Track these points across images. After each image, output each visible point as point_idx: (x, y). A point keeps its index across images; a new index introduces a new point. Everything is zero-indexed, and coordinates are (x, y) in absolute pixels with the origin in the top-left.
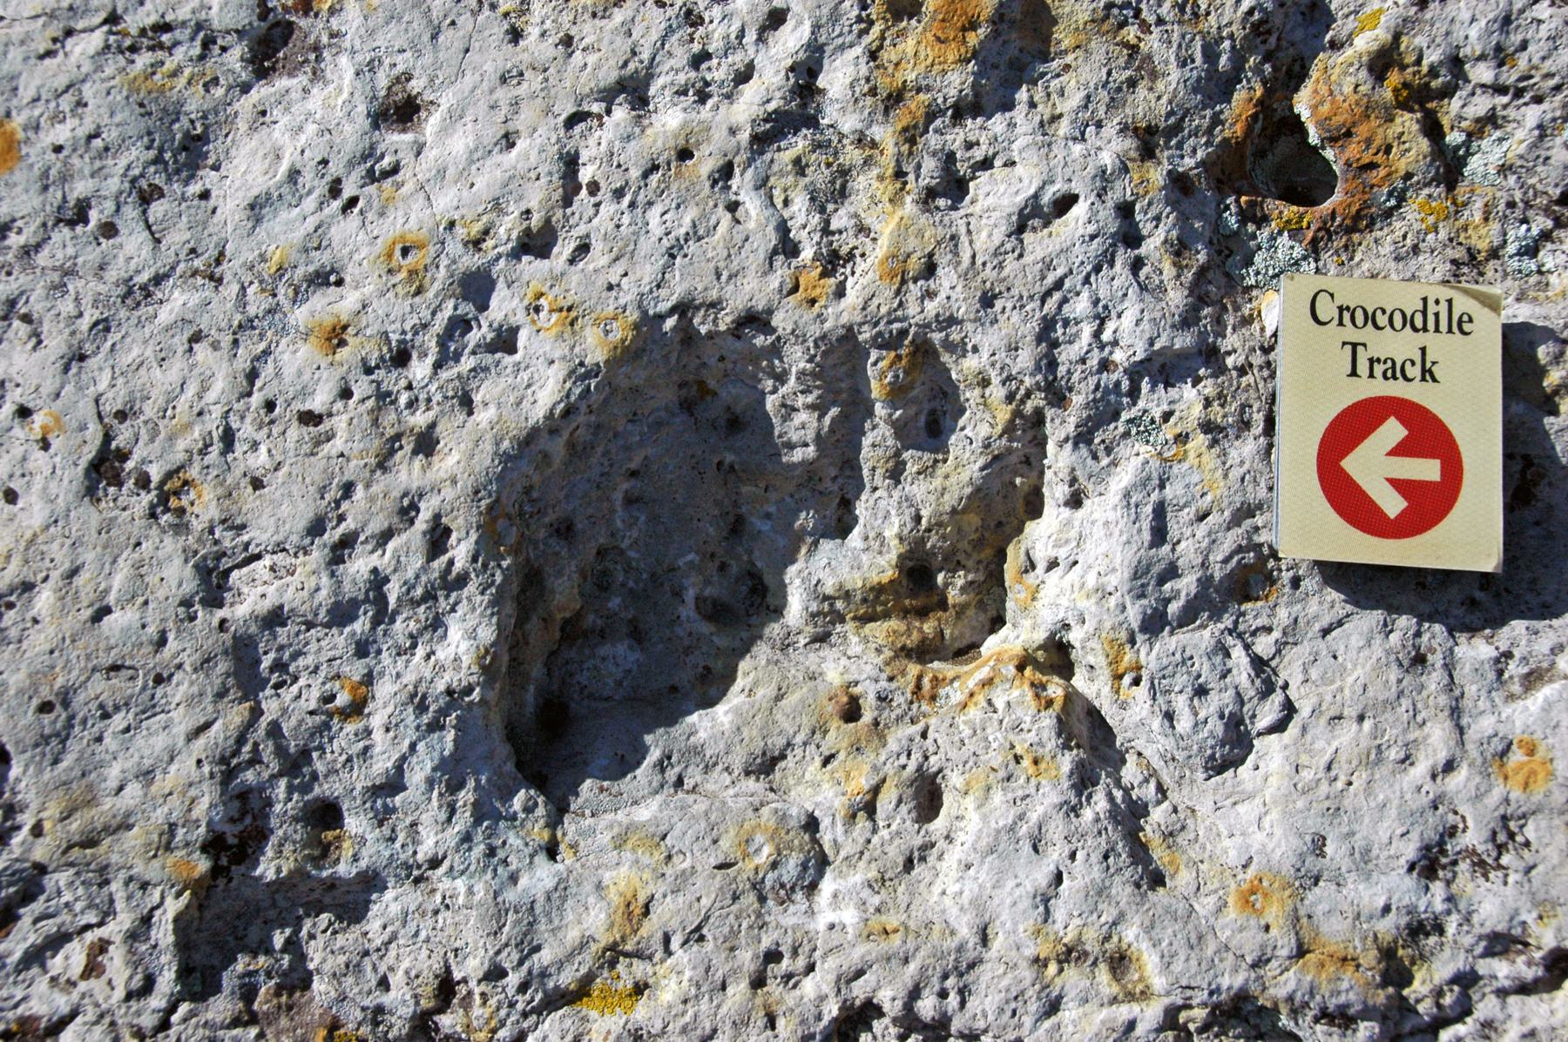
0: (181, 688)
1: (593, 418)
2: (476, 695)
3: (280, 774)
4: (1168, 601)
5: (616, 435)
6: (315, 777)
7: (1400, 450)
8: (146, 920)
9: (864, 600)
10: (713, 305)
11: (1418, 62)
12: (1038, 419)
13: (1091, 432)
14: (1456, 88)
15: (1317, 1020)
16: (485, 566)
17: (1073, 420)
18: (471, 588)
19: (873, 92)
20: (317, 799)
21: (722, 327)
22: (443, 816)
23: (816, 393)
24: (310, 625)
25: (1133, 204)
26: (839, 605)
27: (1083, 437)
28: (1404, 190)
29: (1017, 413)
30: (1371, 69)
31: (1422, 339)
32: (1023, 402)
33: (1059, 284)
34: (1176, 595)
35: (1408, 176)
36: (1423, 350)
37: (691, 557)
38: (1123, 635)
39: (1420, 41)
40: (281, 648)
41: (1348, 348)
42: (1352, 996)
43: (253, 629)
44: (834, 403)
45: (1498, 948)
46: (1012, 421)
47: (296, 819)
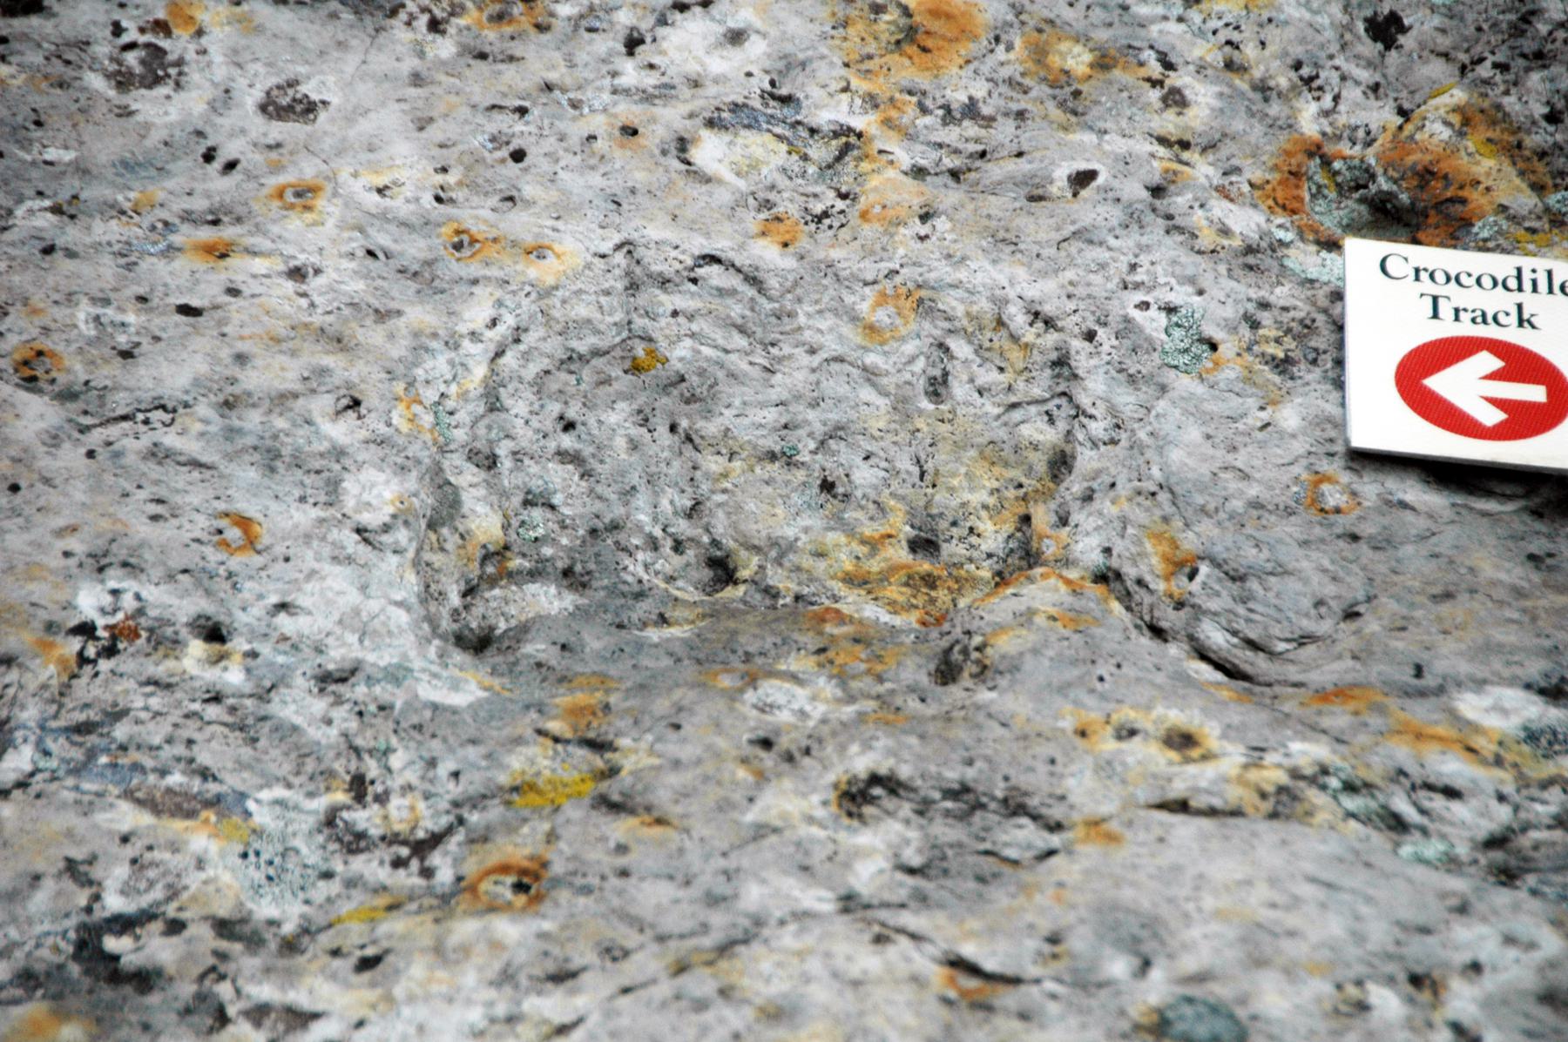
7: (1494, 376)
31: (1517, 297)
36: (1520, 307)
41: (1430, 300)
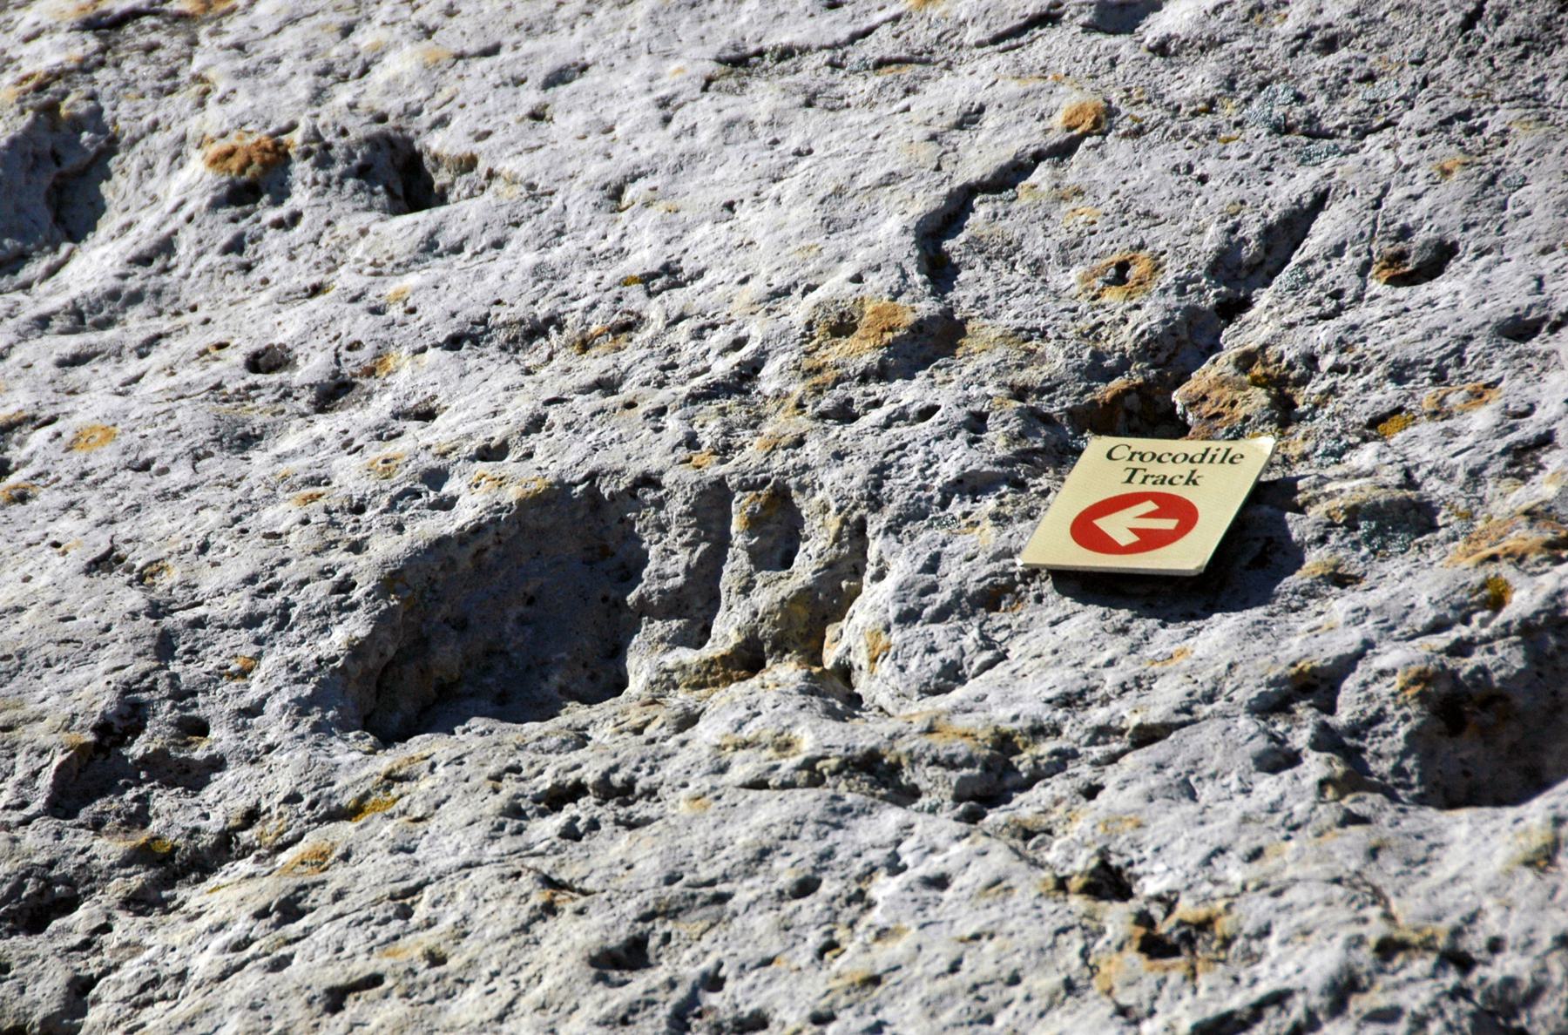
0: (113, 649)
1: (501, 550)
2: (339, 664)
3: (169, 697)
4: (925, 606)
5: (519, 567)
6: (195, 705)
8: (35, 774)
9: (698, 672)
10: (617, 472)
11: (1280, 360)
12: (862, 524)
13: (900, 525)
14: (1311, 377)
15: (929, 765)
16: (375, 600)
17: (885, 520)
18: (360, 611)
19: (798, 368)
20: (192, 718)
21: (622, 487)
22: (288, 726)
23: (691, 532)
24: (224, 628)
25: (987, 414)
26: (676, 676)
27: (893, 529)
28: (1243, 429)
29: (845, 522)
30: (1236, 364)
31: (1193, 467)
32: (850, 513)
33: (902, 447)
34: (932, 602)
35: (1247, 418)
37: (564, 654)
38: (881, 625)
39: (1284, 347)
40: (197, 639)
42: (961, 750)
43: (180, 626)
44: (705, 540)
45: (1101, 739)
46: (840, 530)
47: (171, 724)
